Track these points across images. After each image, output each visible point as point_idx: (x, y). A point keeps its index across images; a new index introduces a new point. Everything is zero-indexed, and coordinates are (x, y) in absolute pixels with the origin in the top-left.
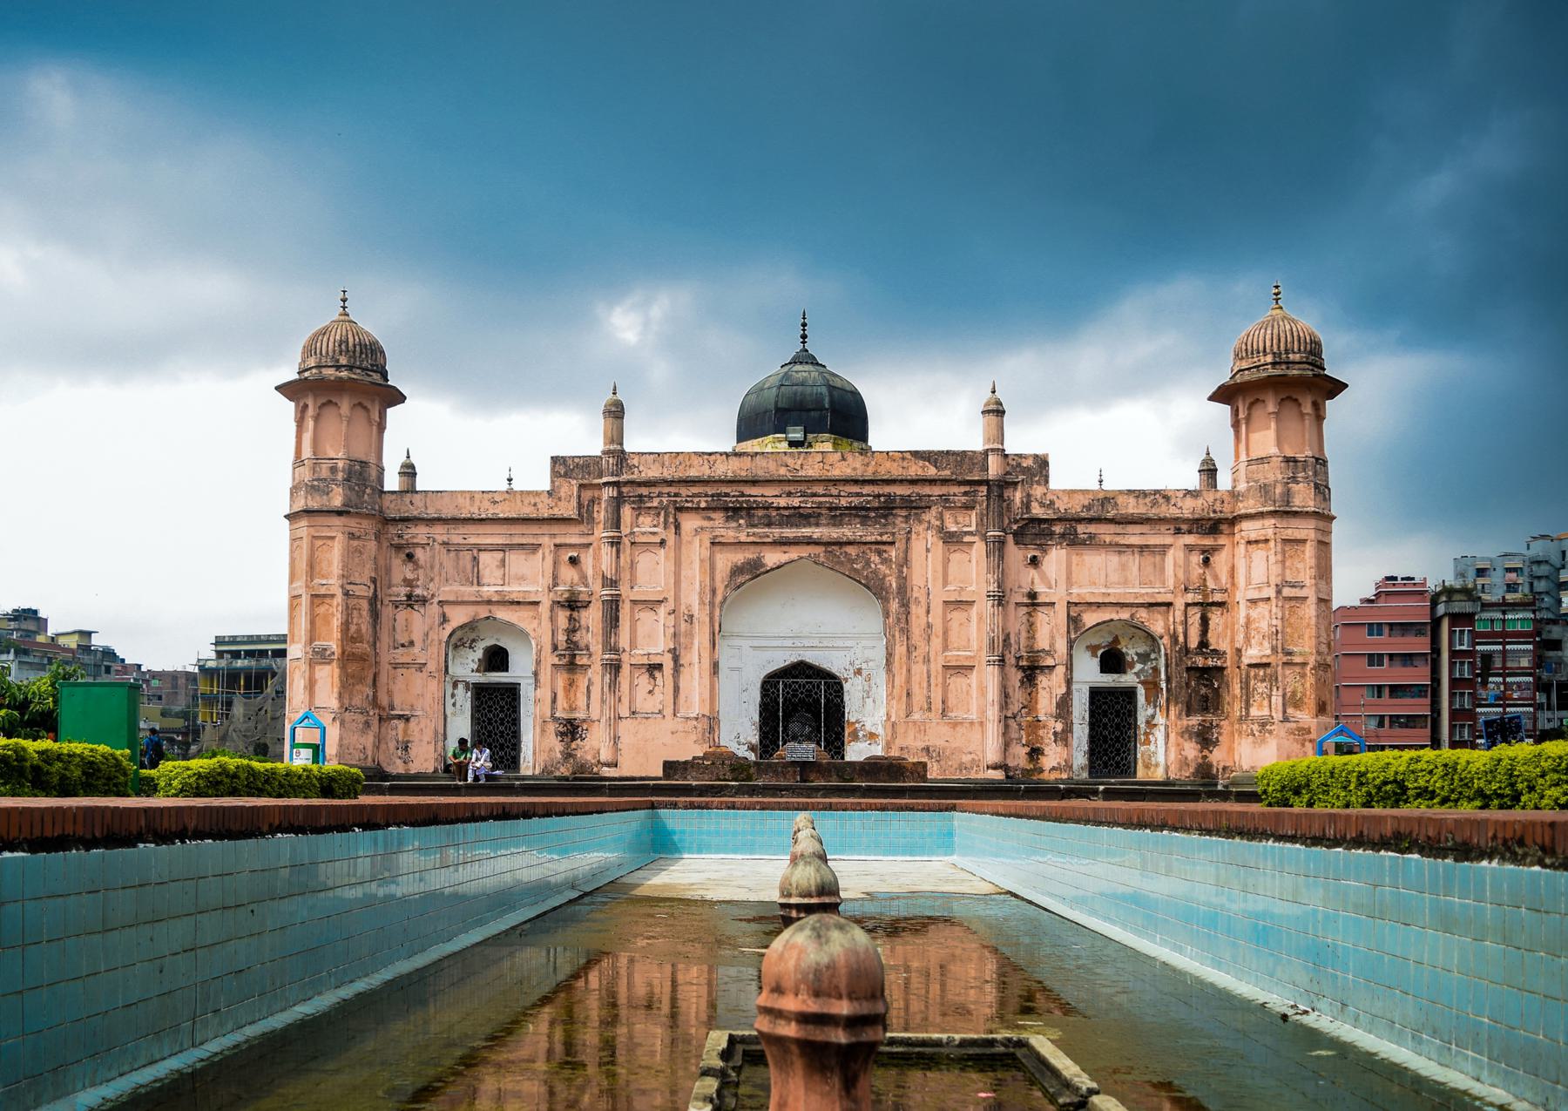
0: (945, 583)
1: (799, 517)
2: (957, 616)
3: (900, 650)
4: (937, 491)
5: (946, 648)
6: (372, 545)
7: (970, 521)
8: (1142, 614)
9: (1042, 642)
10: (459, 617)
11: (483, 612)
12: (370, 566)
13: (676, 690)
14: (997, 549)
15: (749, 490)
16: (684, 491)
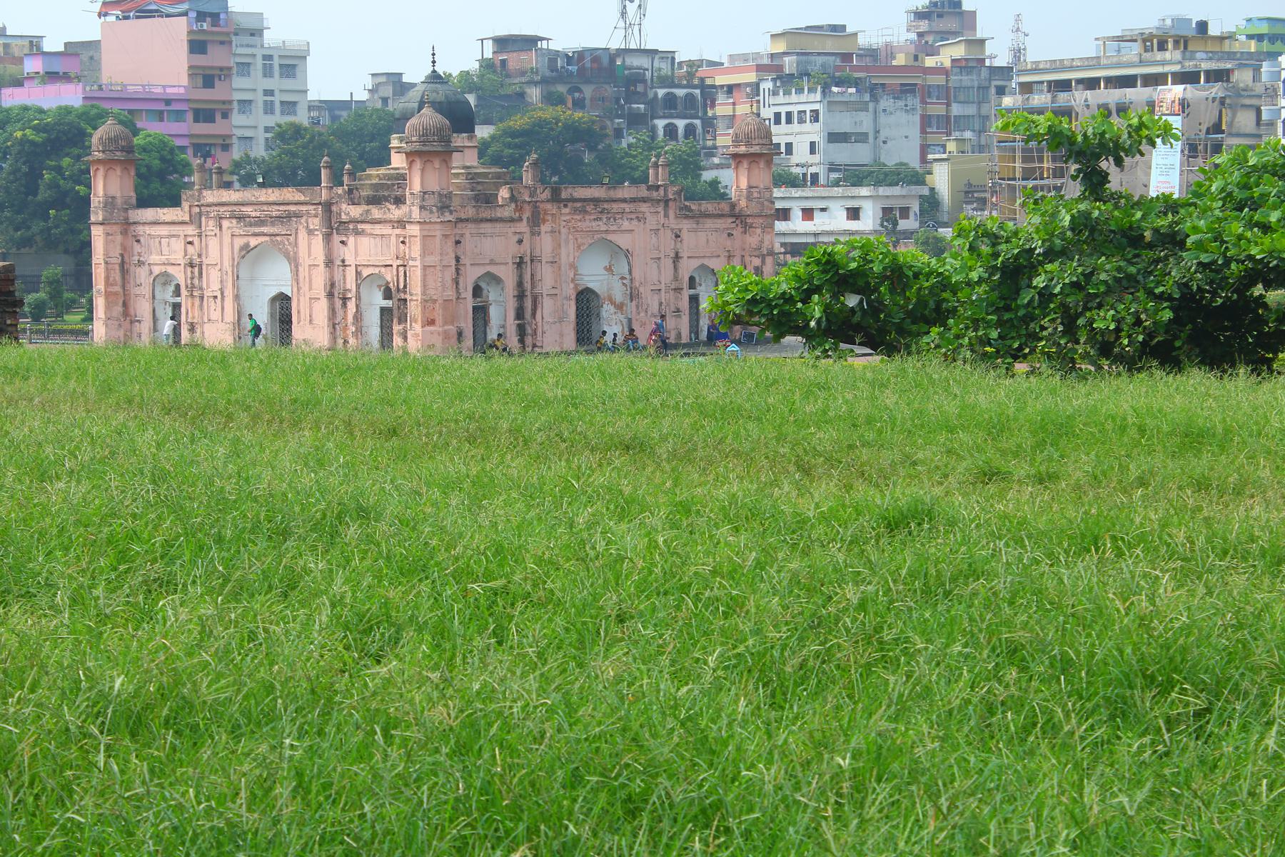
0: (309, 255)
1: (261, 222)
2: (314, 272)
3: (295, 289)
4: (304, 208)
5: (310, 289)
6: (119, 238)
7: (317, 221)
8: (383, 270)
9: (348, 287)
10: (157, 270)
11: (163, 269)
12: (119, 247)
13: (223, 308)
14: (328, 237)
15: (244, 209)
16: (222, 209)
